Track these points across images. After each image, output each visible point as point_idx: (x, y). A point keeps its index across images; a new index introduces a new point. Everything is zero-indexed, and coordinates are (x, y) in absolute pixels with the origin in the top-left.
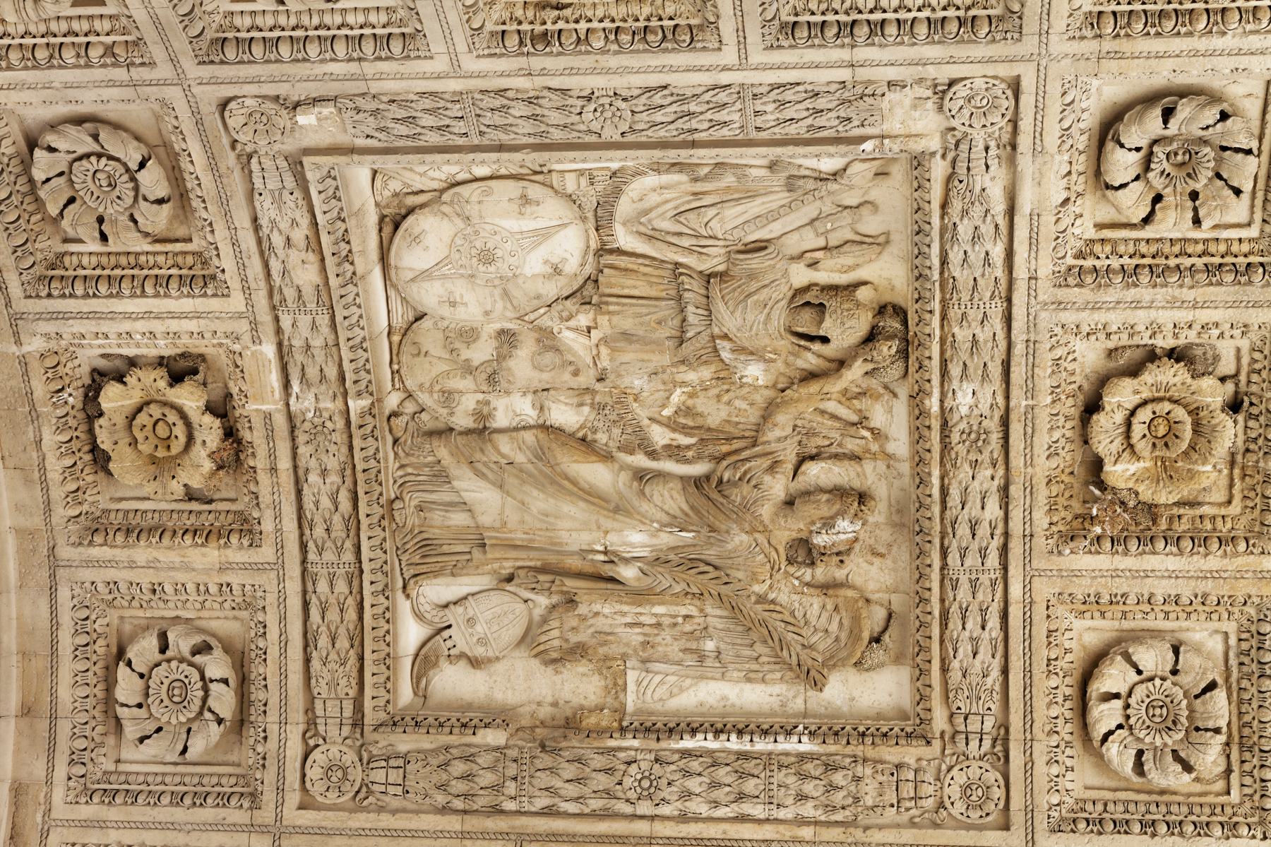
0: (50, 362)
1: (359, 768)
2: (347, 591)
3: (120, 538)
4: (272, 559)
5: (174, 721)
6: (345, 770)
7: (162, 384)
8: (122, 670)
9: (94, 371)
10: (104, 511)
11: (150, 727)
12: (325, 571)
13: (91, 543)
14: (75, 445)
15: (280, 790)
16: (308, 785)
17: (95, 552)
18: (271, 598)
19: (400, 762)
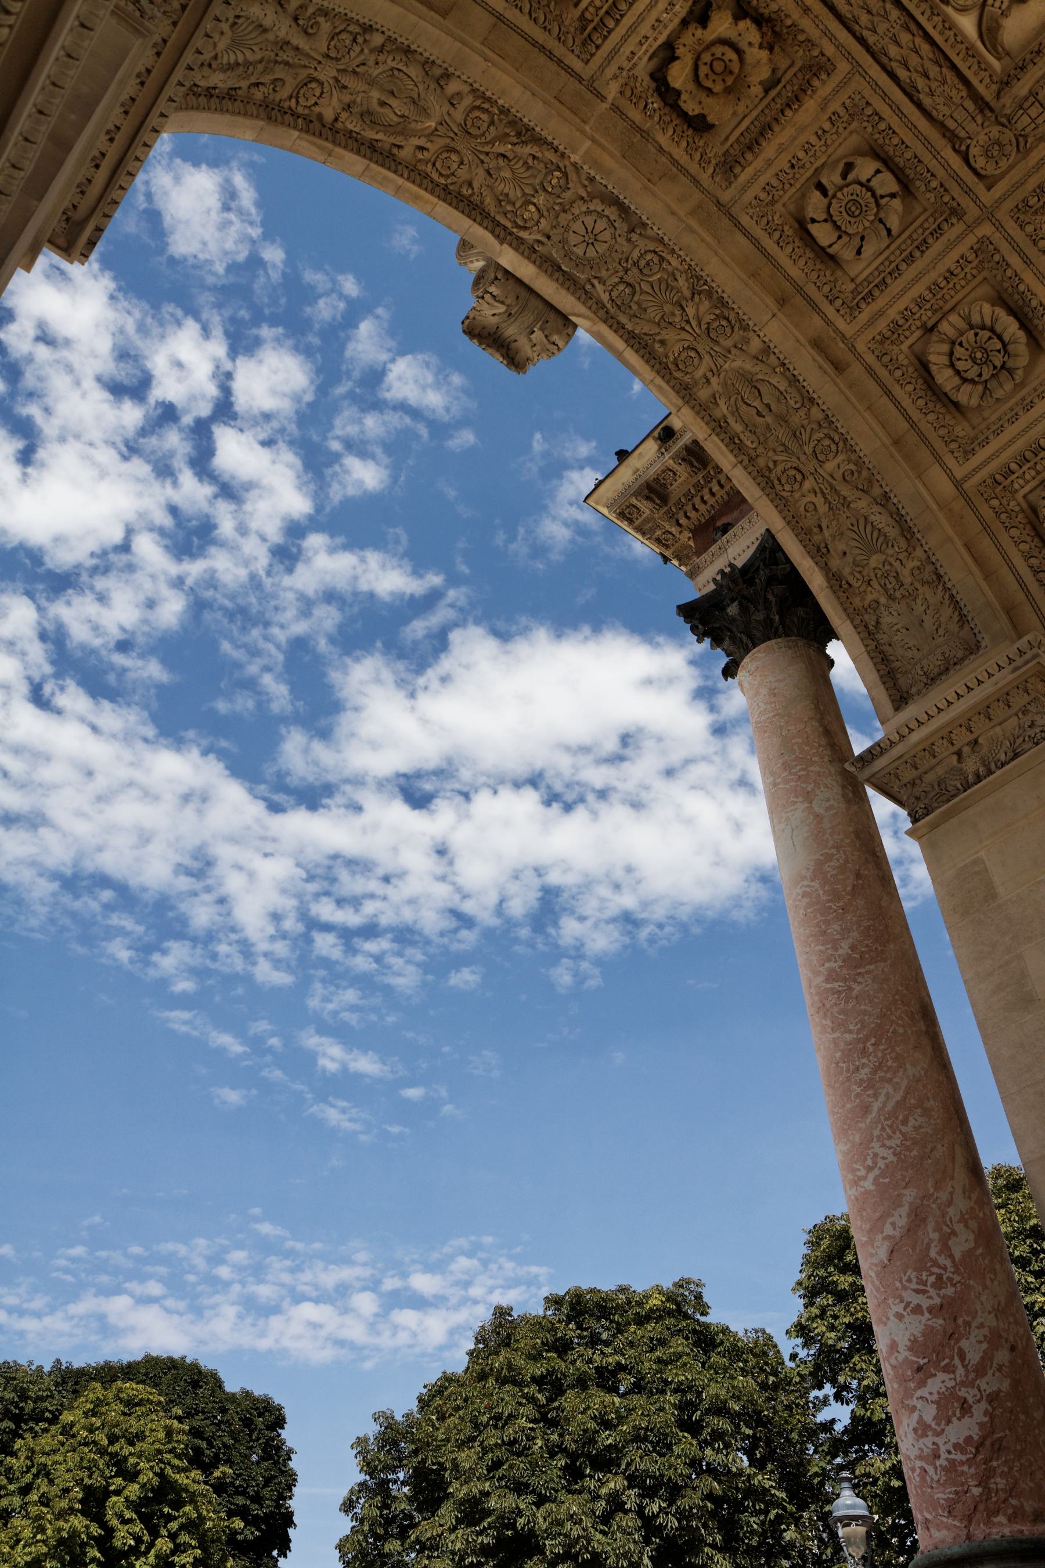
0: (628, 93)
1: (1007, 131)
2: (910, 37)
3: (749, 156)
4: (849, 67)
5: (867, 224)
6: (998, 142)
7: (699, 32)
8: (813, 229)
9: (652, 76)
10: (724, 155)
11: (857, 241)
12: (887, 39)
13: (736, 177)
14: (679, 130)
15: (968, 191)
16: (983, 172)
17: (743, 178)
18: (867, 93)
19: (1032, 99)
